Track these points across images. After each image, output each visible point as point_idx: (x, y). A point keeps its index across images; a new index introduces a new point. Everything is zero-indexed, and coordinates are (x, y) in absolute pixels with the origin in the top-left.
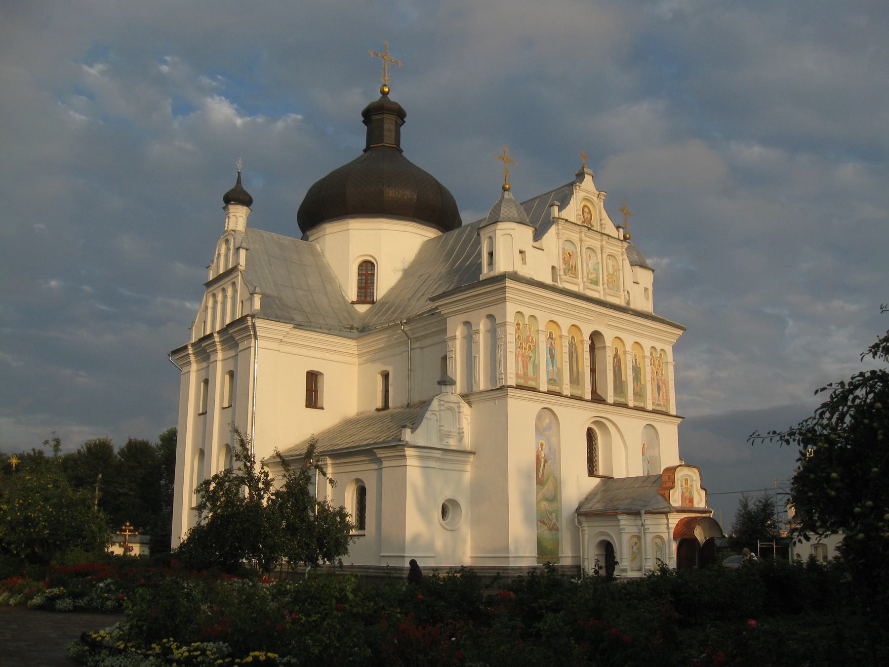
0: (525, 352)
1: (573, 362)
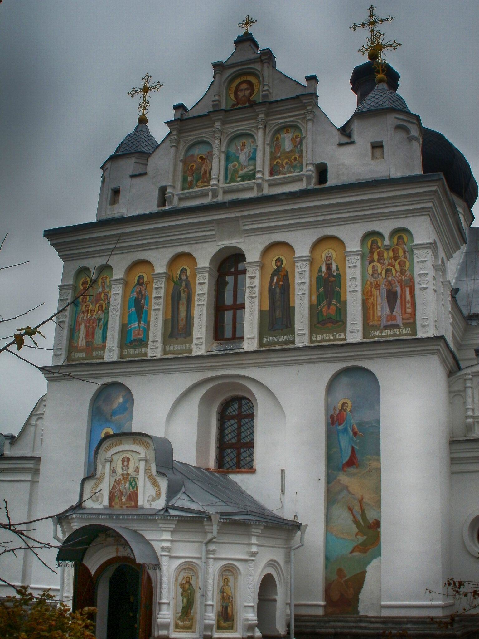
0: (92, 316)
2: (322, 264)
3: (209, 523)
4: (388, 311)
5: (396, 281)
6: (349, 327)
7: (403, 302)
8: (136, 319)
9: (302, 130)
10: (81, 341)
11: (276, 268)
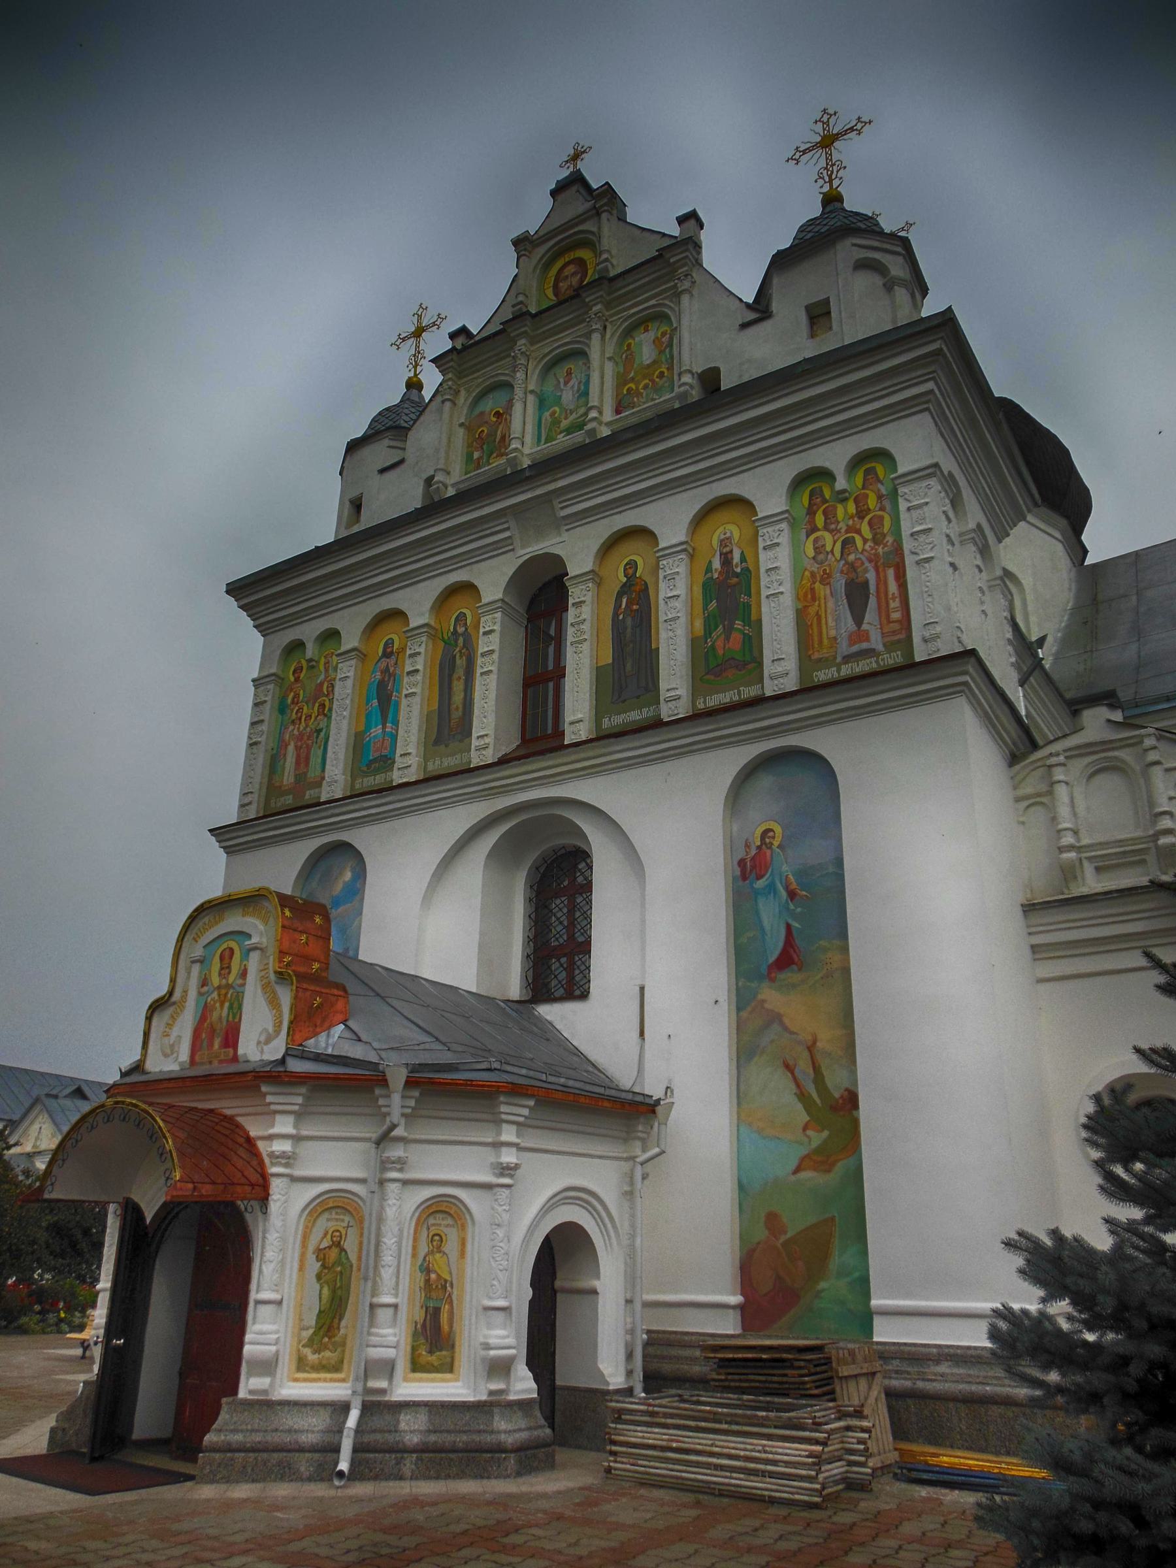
1: (455, 683)
2: (714, 556)
3: (384, 1092)
4: (849, 623)
5: (864, 558)
6: (768, 668)
7: (883, 600)
8: (379, 717)
9: (673, 318)
10: (288, 777)
11: (625, 580)
